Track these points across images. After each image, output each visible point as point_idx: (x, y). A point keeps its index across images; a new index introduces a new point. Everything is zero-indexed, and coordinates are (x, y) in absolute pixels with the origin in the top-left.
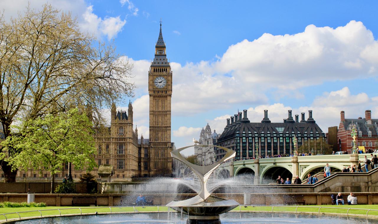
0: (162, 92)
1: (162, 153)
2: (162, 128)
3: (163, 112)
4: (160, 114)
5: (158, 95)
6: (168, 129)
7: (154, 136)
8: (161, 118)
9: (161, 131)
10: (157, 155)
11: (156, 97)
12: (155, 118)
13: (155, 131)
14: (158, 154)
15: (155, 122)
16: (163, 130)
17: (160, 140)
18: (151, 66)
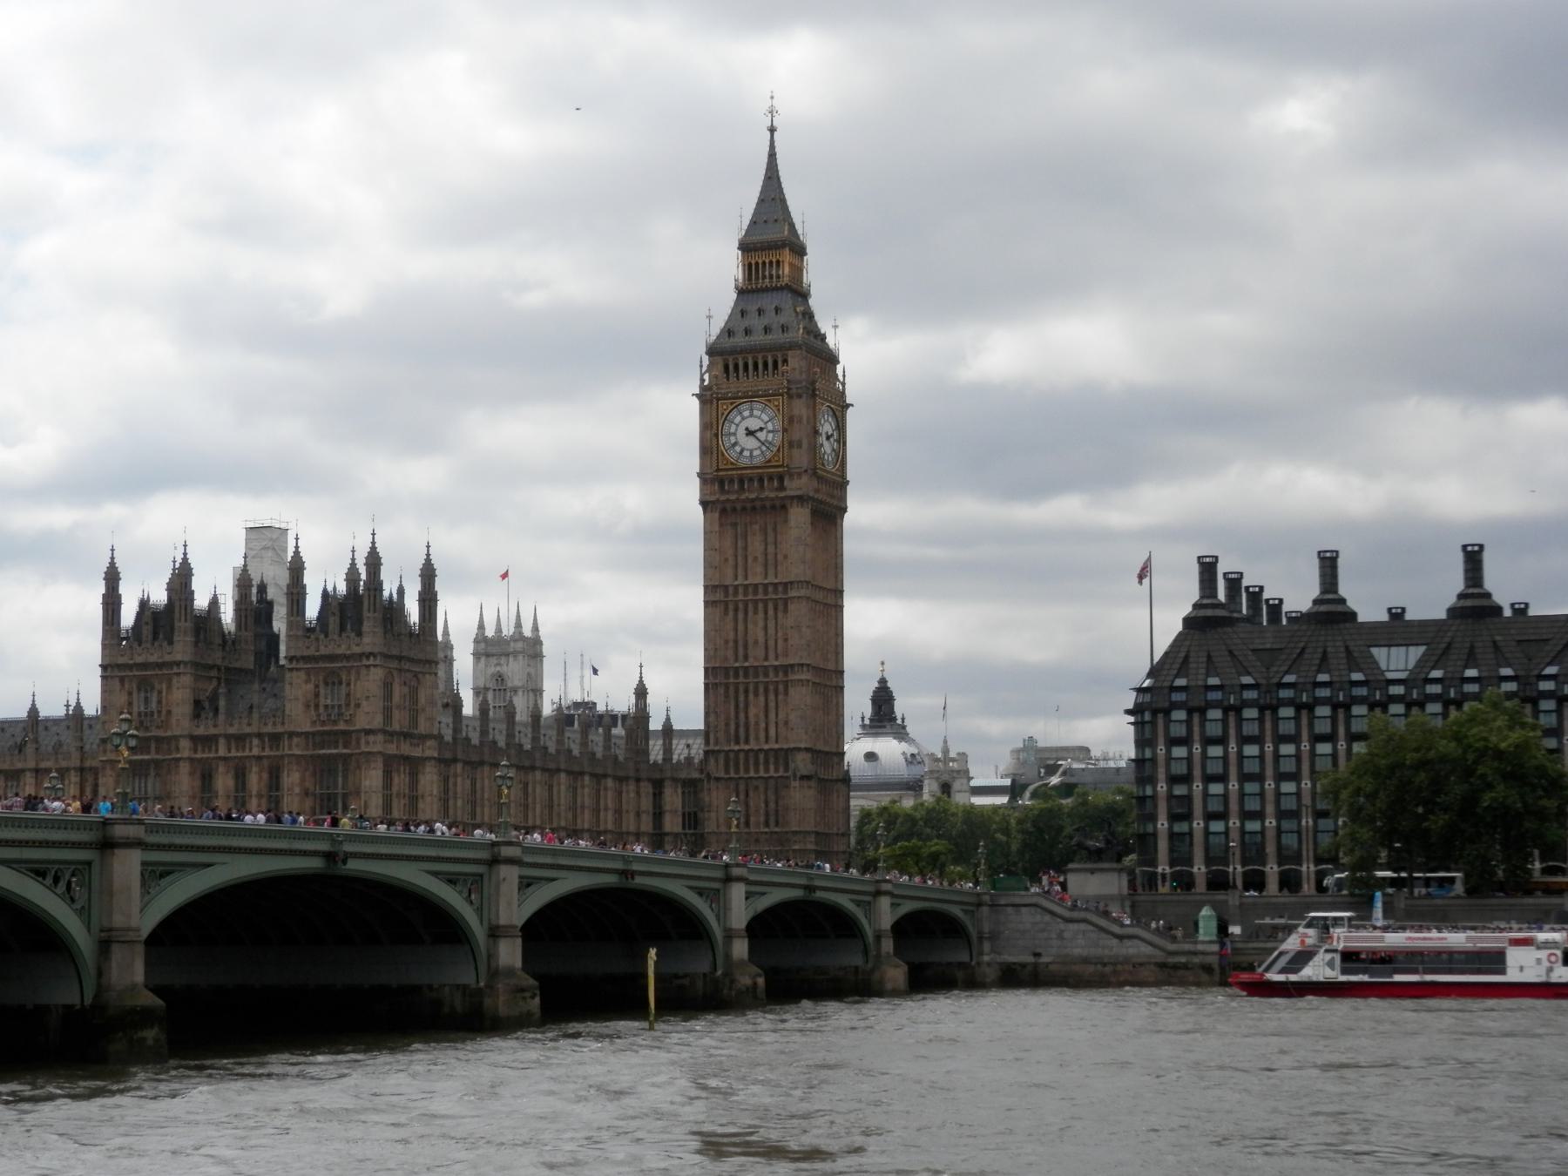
0: (762, 486)
1: (767, 803)
2: (766, 675)
3: (770, 589)
8: (761, 624)
9: (761, 690)
11: (734, 510)
15: (731, 644)
17: (757, 738)
18: (712, 351)
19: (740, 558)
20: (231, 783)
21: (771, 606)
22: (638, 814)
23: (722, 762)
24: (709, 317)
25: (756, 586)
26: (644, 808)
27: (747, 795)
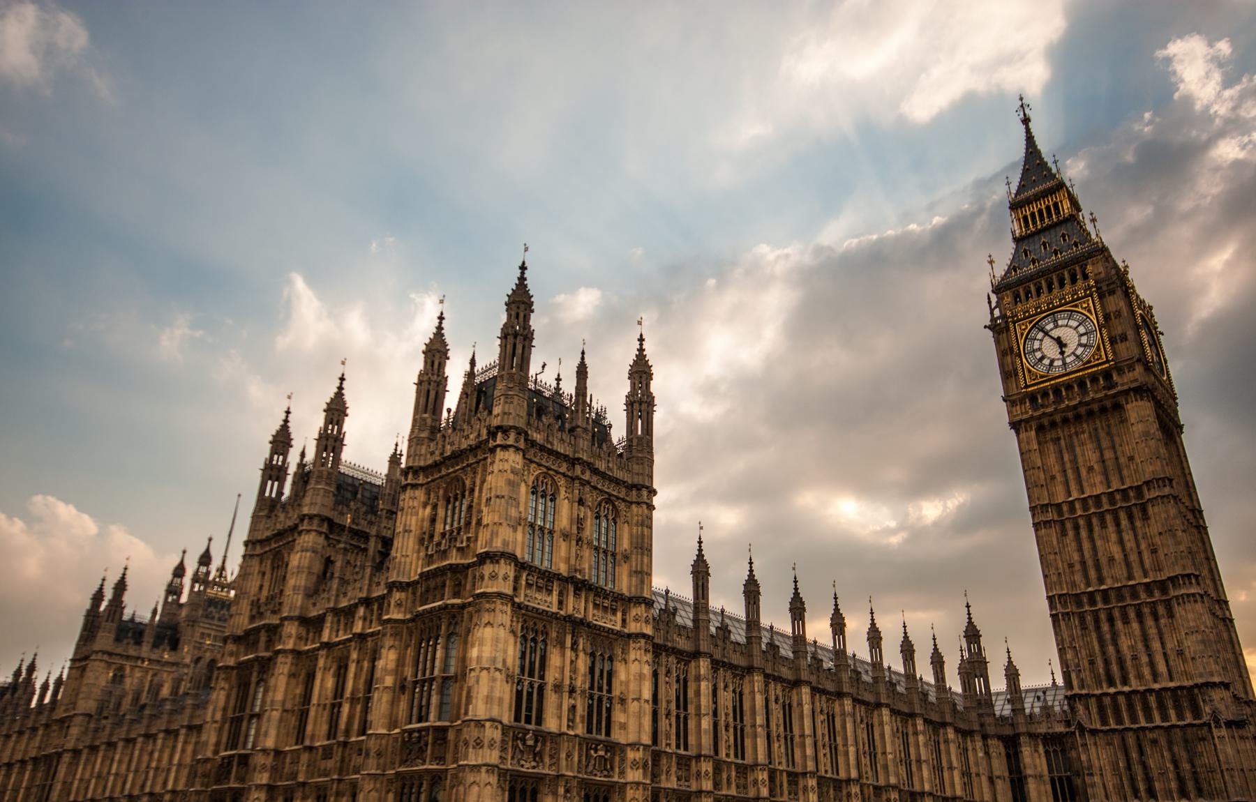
1: (1175, 763)
2: (1135, 595)
3: (1118, 497)
4: (1101, 517)
5: (1063, 411)
6: (1183, 591)
7: (1091, 654)
8: (1114, 537)
9: (1132, 615)
10: (1142, 787)
12: (1074, 544)
13: (1089, 618)
14: (1149, 780)
15: (1078, 567)
16: (1146, 610)
17: (1140, 677)
19: (1070, 472)
20: (330, 683)
21: (1122, 515)
22: (991, 780)
23: (1094, 710)
24: (991, 262)
25: (1098, 497)
26: (997, 773)
27: (1141, 752)
